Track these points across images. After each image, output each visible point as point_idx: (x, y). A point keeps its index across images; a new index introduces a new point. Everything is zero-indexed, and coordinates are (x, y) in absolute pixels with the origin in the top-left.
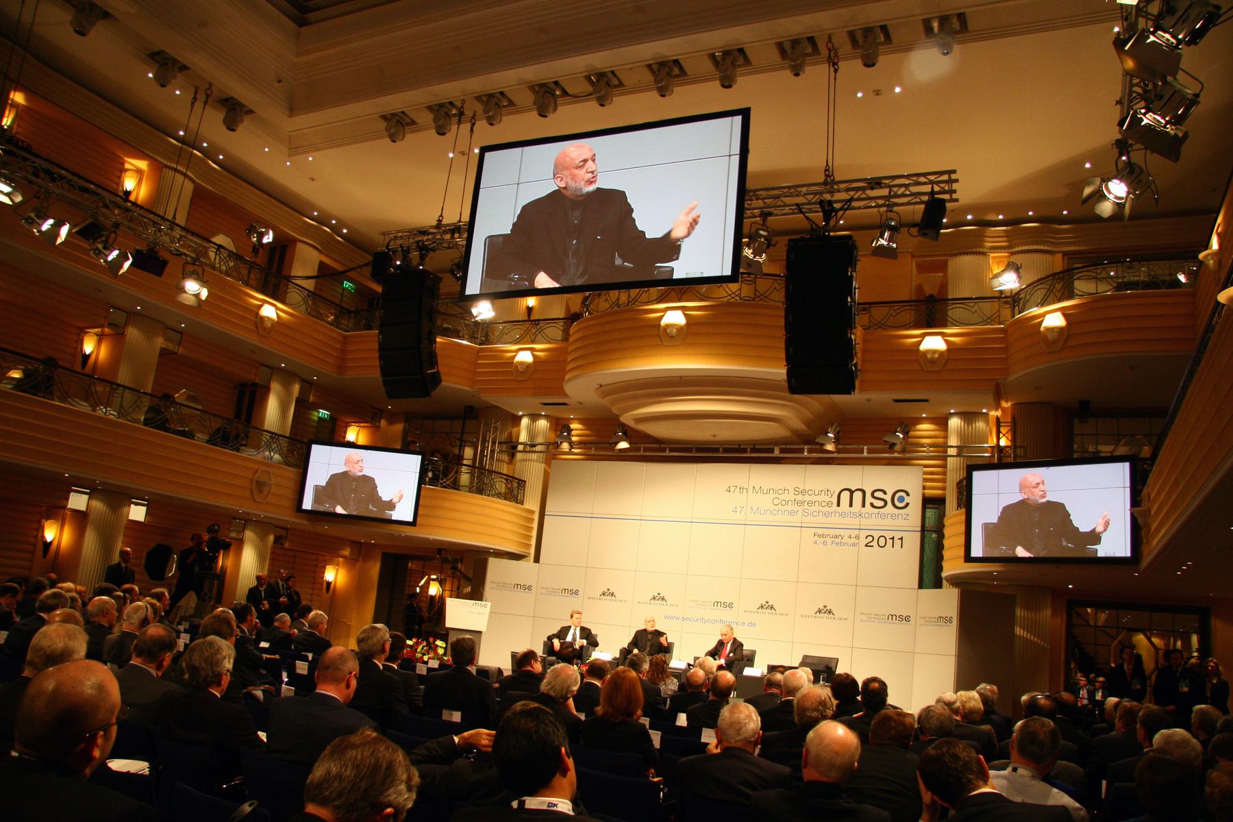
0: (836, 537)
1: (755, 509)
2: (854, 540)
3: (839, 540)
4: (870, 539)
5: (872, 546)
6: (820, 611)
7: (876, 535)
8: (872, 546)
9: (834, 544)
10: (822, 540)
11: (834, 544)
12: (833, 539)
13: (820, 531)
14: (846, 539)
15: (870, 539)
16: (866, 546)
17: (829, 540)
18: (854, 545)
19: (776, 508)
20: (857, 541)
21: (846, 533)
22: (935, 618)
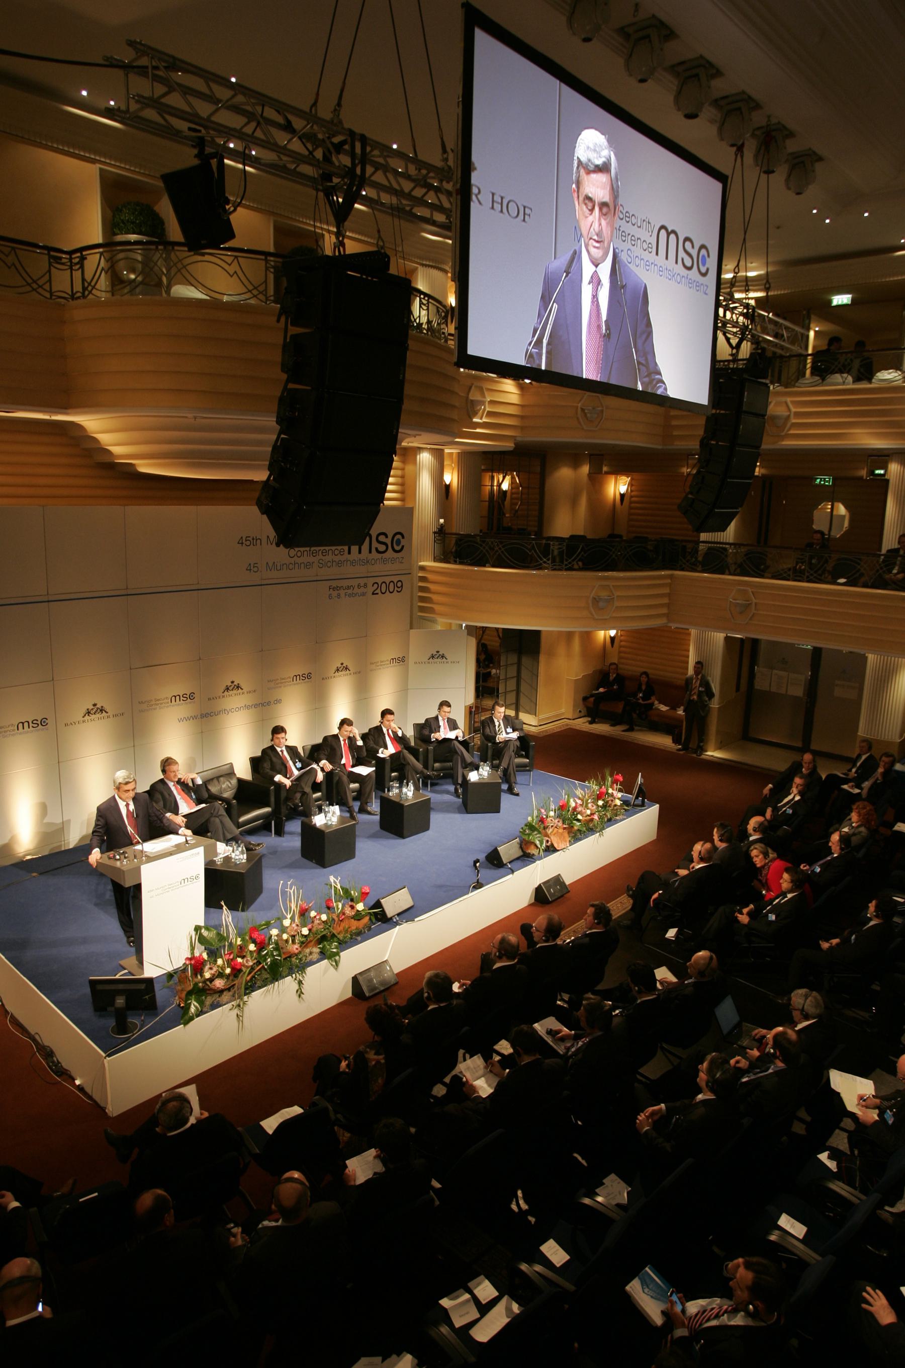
0: (348, 588)
1: (271, 565)
2: (362, 590)
3: (350, 591)
4: (376, 586)
5: (377, 594)
6: (338, 670)
7: (380, 580)
8: (377, 594)
9: (347, 596)
10: (336, 592)
11: (347, 596)
12: (346, 591)
13: (334, 584)
14: (356, 590)
15: (376, 586)
16: (373, 594)
17: (342, 592)
18: (364, 594)
19: (292, 561)
20: (365, 590)
21: (355, 582)
22: (388, 660)
